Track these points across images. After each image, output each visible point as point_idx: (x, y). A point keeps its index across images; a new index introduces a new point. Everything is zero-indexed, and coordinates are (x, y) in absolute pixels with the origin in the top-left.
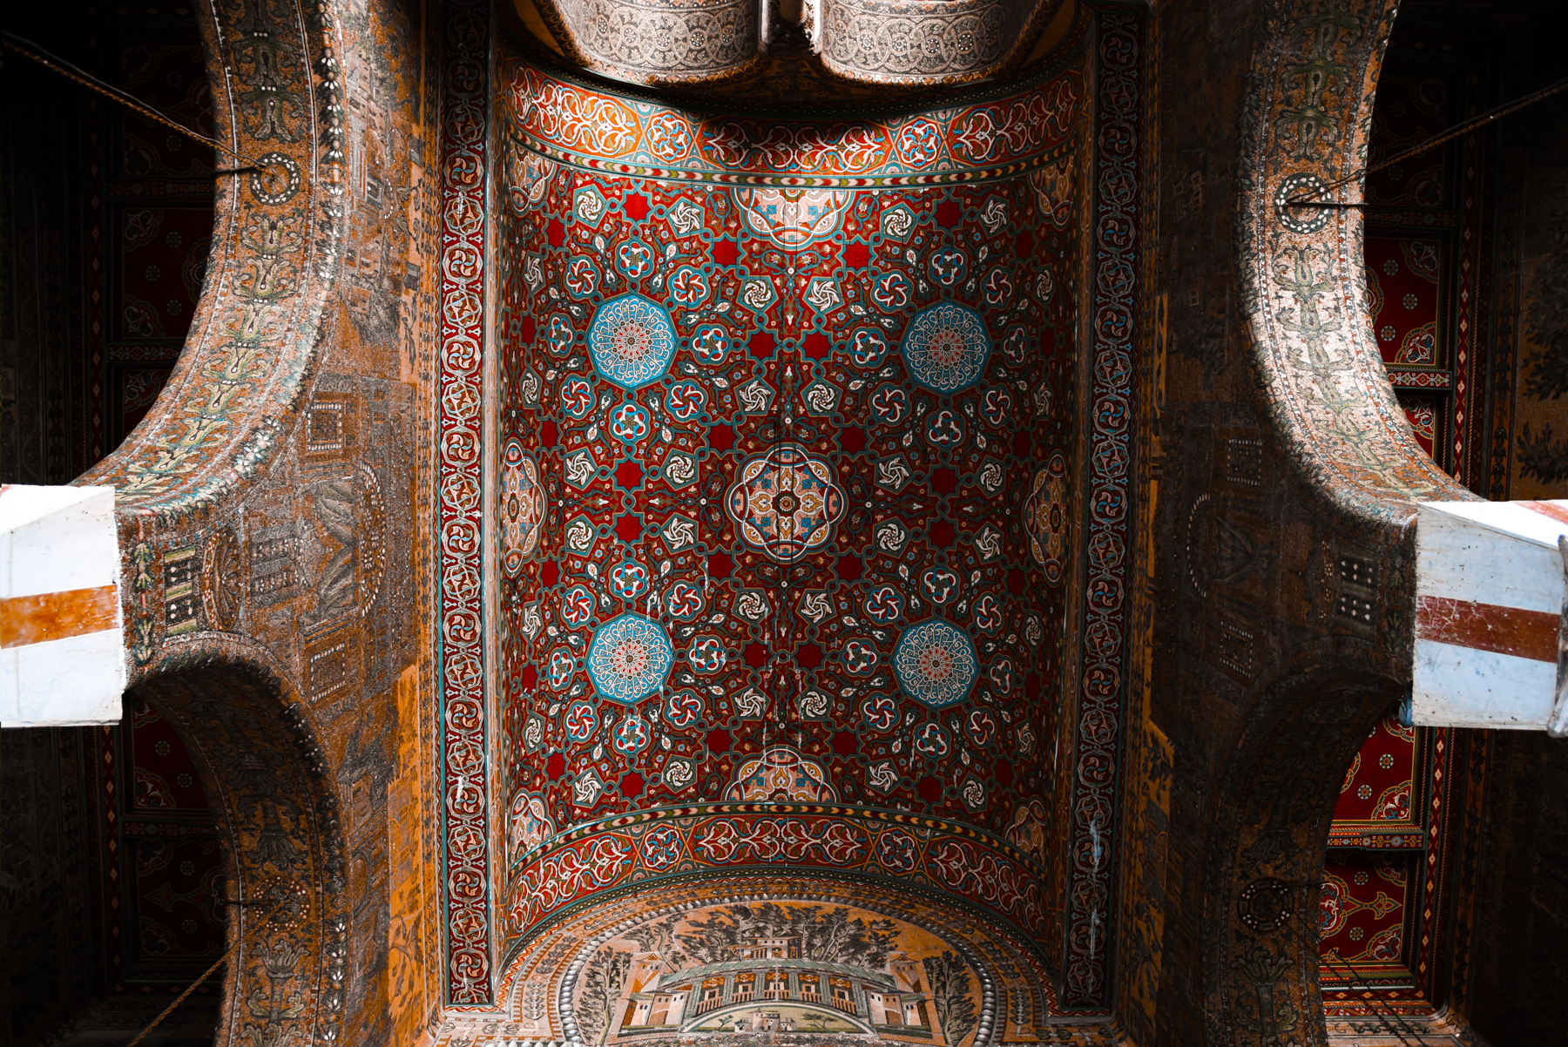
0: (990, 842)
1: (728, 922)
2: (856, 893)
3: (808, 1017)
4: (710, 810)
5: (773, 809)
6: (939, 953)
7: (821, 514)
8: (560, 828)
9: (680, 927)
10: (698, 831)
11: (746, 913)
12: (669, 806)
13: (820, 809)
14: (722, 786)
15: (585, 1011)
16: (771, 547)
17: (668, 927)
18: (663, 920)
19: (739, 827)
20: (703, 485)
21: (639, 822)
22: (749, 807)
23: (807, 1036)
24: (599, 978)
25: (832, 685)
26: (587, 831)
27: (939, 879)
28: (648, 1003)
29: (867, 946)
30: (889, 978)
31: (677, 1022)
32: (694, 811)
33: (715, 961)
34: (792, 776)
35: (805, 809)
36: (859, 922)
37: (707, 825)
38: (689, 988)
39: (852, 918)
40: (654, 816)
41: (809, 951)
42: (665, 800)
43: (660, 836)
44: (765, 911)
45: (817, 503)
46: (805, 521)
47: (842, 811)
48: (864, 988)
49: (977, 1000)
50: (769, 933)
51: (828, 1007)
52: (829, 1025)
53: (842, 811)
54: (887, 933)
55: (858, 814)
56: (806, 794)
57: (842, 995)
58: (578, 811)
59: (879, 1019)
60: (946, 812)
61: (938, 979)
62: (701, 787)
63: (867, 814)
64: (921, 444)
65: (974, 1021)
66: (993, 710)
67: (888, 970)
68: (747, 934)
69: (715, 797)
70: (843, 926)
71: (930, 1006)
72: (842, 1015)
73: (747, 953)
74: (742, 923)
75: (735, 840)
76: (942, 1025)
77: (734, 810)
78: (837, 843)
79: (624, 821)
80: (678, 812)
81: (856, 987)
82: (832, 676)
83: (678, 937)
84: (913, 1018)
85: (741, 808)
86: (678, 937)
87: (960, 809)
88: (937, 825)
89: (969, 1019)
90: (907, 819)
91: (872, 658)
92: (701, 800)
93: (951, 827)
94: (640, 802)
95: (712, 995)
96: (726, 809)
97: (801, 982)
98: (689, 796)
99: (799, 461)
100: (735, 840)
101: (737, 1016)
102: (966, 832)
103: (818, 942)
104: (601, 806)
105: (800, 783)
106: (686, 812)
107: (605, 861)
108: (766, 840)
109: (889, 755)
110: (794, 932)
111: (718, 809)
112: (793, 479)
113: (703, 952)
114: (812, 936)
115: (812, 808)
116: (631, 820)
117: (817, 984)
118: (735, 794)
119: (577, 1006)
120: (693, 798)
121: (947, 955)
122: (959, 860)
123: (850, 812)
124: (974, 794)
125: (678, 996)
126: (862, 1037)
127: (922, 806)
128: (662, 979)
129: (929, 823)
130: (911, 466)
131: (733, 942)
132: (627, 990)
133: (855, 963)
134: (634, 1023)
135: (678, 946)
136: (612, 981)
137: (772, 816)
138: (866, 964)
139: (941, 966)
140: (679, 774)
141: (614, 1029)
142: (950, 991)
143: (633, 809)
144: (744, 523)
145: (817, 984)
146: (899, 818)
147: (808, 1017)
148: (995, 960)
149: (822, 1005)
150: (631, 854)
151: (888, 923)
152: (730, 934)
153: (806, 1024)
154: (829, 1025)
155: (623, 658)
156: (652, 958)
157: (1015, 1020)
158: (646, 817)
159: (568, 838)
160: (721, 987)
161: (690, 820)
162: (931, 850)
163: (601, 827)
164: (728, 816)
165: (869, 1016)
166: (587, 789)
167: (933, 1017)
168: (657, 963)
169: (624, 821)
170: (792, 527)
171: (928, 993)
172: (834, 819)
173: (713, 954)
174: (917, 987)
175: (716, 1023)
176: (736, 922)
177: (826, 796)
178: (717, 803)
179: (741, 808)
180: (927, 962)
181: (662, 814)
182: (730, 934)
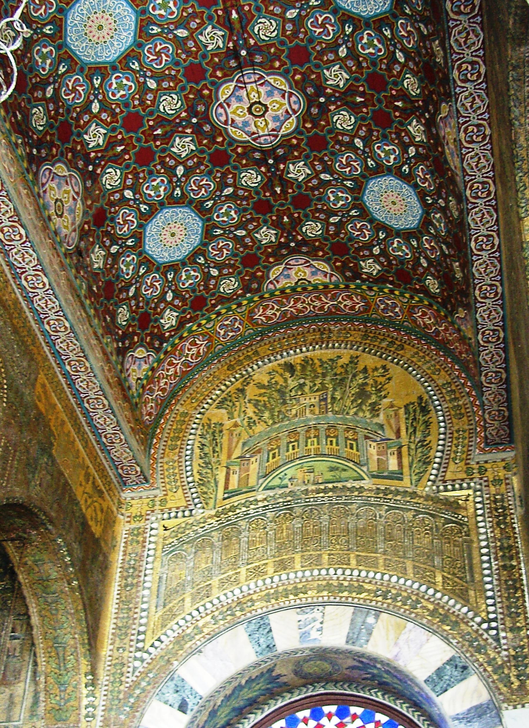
0: (446, 316)
1: (281, 381)
2: (365, 336)
3: (332, 469)
4: (256, 299)
5: (299, 289)
6: (414, 399)
7: (287, 112)
8: (158, 350)
9: (251, 391)
10: (251, 312)
11: (290, 368)
12: (226, 305)
13: (332, 286)
14: (260, 284)
15: (202, 483)
16: (254, 140)
17: (242, 391)
18: (238, 385)
19: (279, 303)
20: (192, 111)
21: (209, 320)
22: (283, 291)
23: (330, 486)
24: (206, 450)
25: (322, 216)
26: (177, 341)
27: (419, 326)
28: (237, 468)
29: (369, 397)
30: (381, 427)
31: (255, 483)
32: (245, 302)
33: (275, 423)
34: (308, 271)
35: (321, 287)
36: (365, 370)
37: (256, 307)
38: (259, 451)
39: (361, 367)
40: (219, 314)
41: (332, 404)
42: (222, 303)
43: (226, 323)
44: (306, 361)
45: (282, 105)
46: (276, 119)
47: (347, 287)
48: (367, 438)
49: (434, 445)
50: (307, 389)
51: (343, 459)
52: (344, 475)
53: (347, 287)
54: (382, 380)
55: (358, 287)
56: (319, 279)
57: (352, 448)
58: (167, 334)
59: (373, 466)
60: (417, 291)
61: (412, 425)
62: (247, 289)
63: (364, 287)
64: (353, 54)
65: (429, 463)
66: (436, 237)
67: (381, 419)
68: (293, 393)
69: (258, 290)
70: (354, 376)
71: (405, 450)
72: (351, 465)
73: (294, 412)
74: (290, 381)
75: (277, 310)
76: (410, 467)
77: (272, 294)
78: (349, 303)
79: (199, 325)
80: (234, 307)
81: (360, 436)
82: (321, 211)
83: (250, 401)
84: (393, 464)
85: (277, 293)
86: (250, 401)
87: (425, 291)
88: (412, 297)
89: (427, 462)
90: (392, 292)
91: (347, 198)
92: (248, 295)
93: (421, 301)
94: (206, 310)
95: (274, 457)
96: (267, 296)
97: (328, 436)
98: (240, 295)
99: (259, 79)
100: (277, 310)
101: (290, 473)
102: (431, 305)
103: (338, 395)
104: (181, 323)
105: (313, 274)
106: (239, 305)
107: (195, 350)
108: (299, 305)
109: (372, 255)
110: (323, 387)
111: (261, 297)
112: (258, 92)
113: (267, 415)
114: (335, 390)
115: (326, 286)
116: (204, 322)
117: (336, 437)
118: (271, 286)
119: (197, 477)
120: (243, 295)
121: (420, 398)
122: (430, 319)
123: (353, 286)
124: (433, 284)
125: (253, 459)
126: (362, 483)
127: (400, 285)
128: (244, 444)
129: (407, 295)
130: (349, 70)
131: (284, 403)
132: (223, 457)
133: (361, 414)
134: (231, 488)
135: (250, 411)
136: (214, 452)
137: (300, 293)
138: (368, 414)
139: (415, 411)
140: (229, 286)
141: (220, 495)
142: (419, 435)
143: (203, 315)
144: (229, 127)
145: (336, 437)
146: (386, 290)
147: (332, 469)
148: (451, 400)
149: (339, 457)
150: (210, 340)
151: (384, 367)
152: (281, 392)
153: (328, 476)
154: (344, 475)
155: (168, 234)
156: (236, 425)
157: (454, 459)
158: (214, 316)
159: (166, 353)
160: (278, 447)
161: (244, 308)
162: (411, 310)
163: (185, 335)
164: (269, 299)
165: (367, 464)
166: (169, 319)
167: (406, 461)
168: (239, 429)
169: (199, 325)
170: (267, 124)
171: (404, 438)
172: (342, 290)
173: (272, 417)
174: (398, 433)
175: (276, 482)
176: (286, 380)
177: (334, 279)
178: (259, 294)
179: (277, 293)
180: (406, 407)
181: (224, 311)
182: (281, 392)
